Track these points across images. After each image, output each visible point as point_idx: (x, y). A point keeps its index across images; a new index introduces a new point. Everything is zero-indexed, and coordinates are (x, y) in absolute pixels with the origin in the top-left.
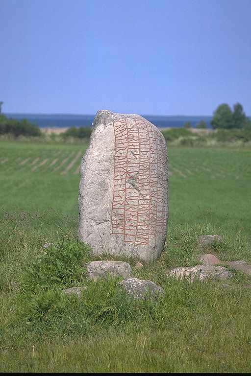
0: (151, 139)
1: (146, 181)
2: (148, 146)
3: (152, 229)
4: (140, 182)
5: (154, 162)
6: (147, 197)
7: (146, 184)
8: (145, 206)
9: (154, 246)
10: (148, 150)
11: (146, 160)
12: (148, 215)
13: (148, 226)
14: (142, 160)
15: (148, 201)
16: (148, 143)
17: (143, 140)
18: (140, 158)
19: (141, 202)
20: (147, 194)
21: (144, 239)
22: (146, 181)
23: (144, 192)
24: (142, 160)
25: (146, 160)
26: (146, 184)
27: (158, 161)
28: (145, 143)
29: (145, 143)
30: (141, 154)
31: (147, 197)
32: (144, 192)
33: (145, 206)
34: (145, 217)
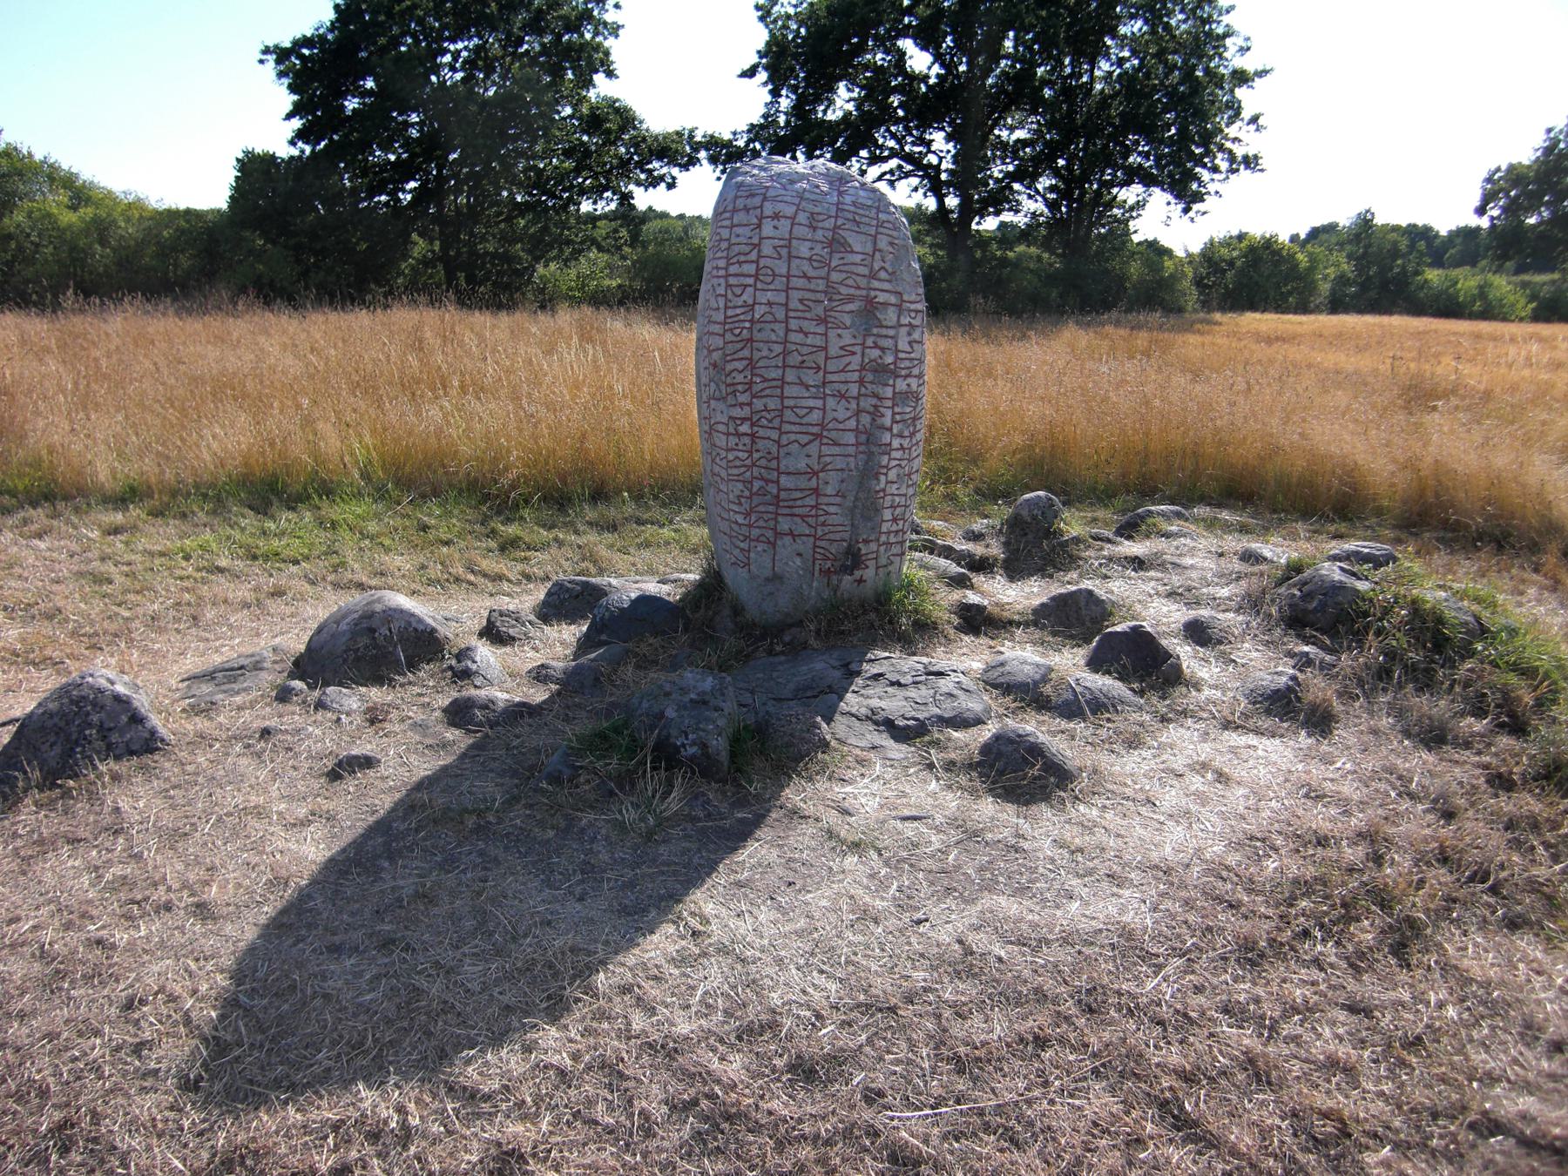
0: (767, 249)
1: (740, 378)
2: (751, 269)
3: (761, 523)
4: (729, 380)
5: (769, 318)
6: (745, 428)
7: (740, 388)
8: (740, 454)
9: (768, 573)
10: (750, 281)
11: (738, 311)
12: (748, 483)
13: (747, 515)
14: (730, 313)
15: (747, 440)
16: (753, 256)
17: (736, 249)
18: (726, 308)
19: (733, 440)
20: (744, 420)
21: (742, 550)
22: (740, 378)
23: (737, 412)
24: (730, 313)
25: (738, 311)
26: (740, 388)
27: (792, 314)
28: (742, 258)
29: (742, 258)
30: (730, 296)
31: (745, 428)
32: (737, 412)
33: (740, 454)
34: (740, 486)
